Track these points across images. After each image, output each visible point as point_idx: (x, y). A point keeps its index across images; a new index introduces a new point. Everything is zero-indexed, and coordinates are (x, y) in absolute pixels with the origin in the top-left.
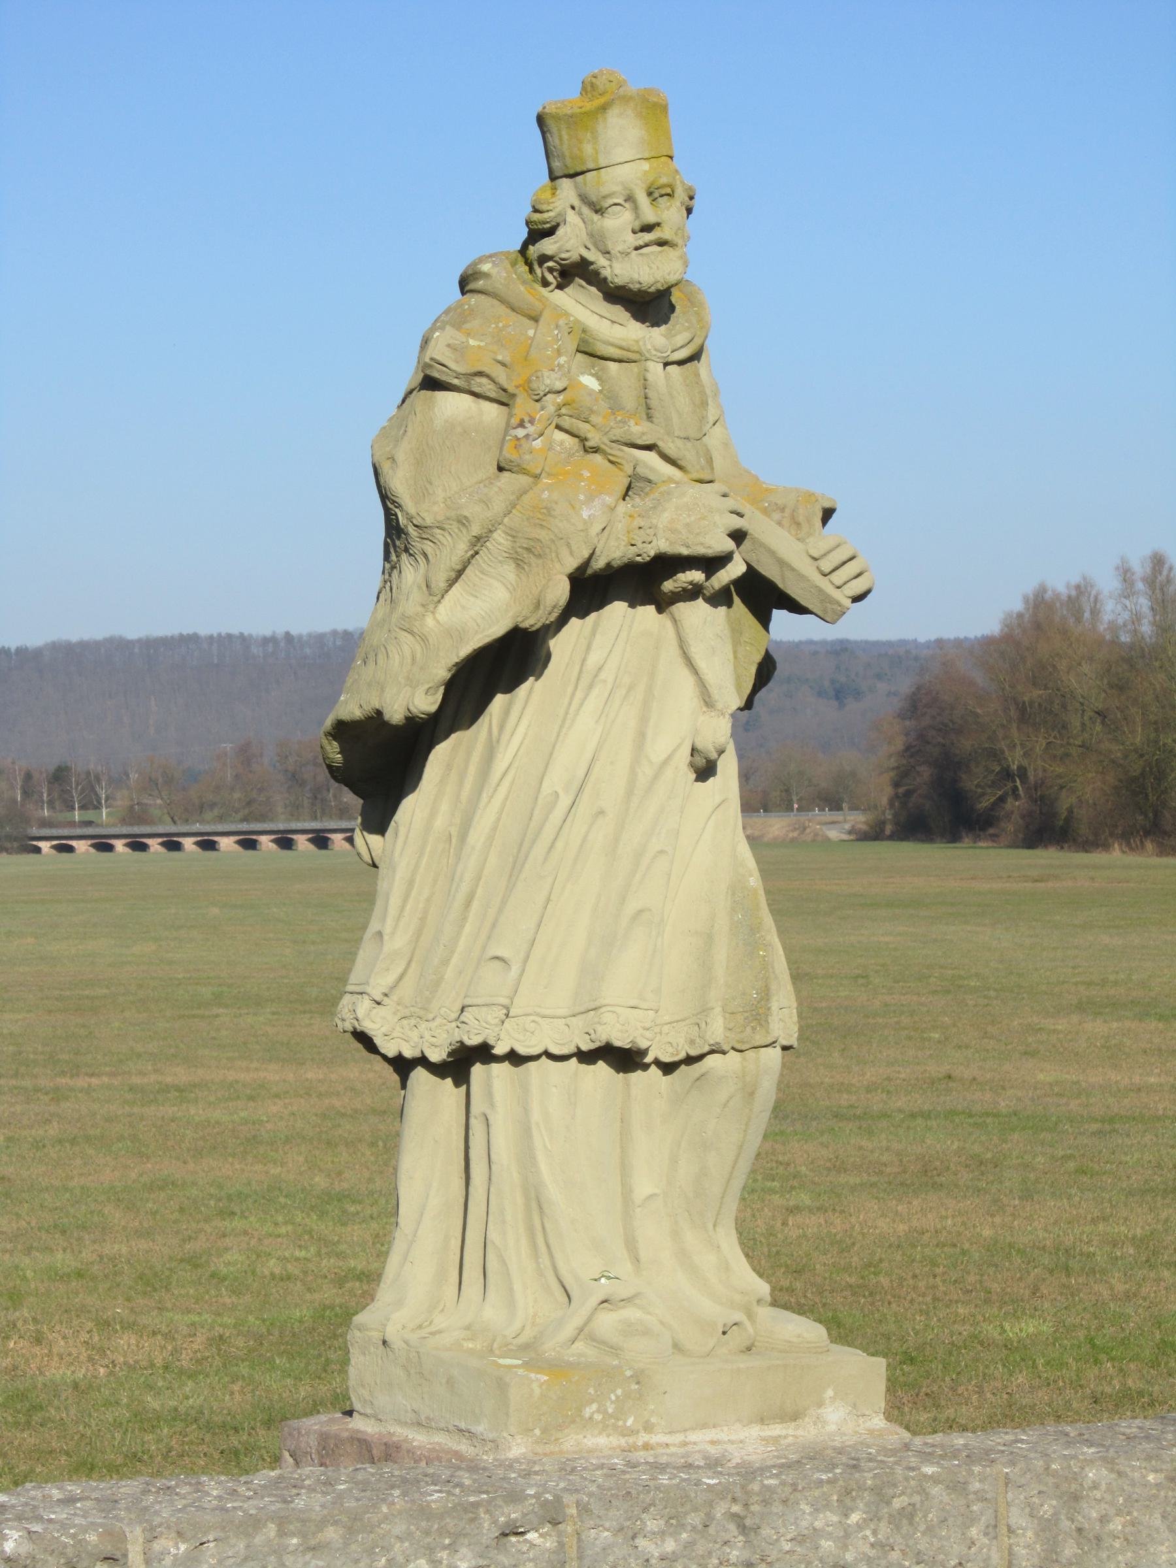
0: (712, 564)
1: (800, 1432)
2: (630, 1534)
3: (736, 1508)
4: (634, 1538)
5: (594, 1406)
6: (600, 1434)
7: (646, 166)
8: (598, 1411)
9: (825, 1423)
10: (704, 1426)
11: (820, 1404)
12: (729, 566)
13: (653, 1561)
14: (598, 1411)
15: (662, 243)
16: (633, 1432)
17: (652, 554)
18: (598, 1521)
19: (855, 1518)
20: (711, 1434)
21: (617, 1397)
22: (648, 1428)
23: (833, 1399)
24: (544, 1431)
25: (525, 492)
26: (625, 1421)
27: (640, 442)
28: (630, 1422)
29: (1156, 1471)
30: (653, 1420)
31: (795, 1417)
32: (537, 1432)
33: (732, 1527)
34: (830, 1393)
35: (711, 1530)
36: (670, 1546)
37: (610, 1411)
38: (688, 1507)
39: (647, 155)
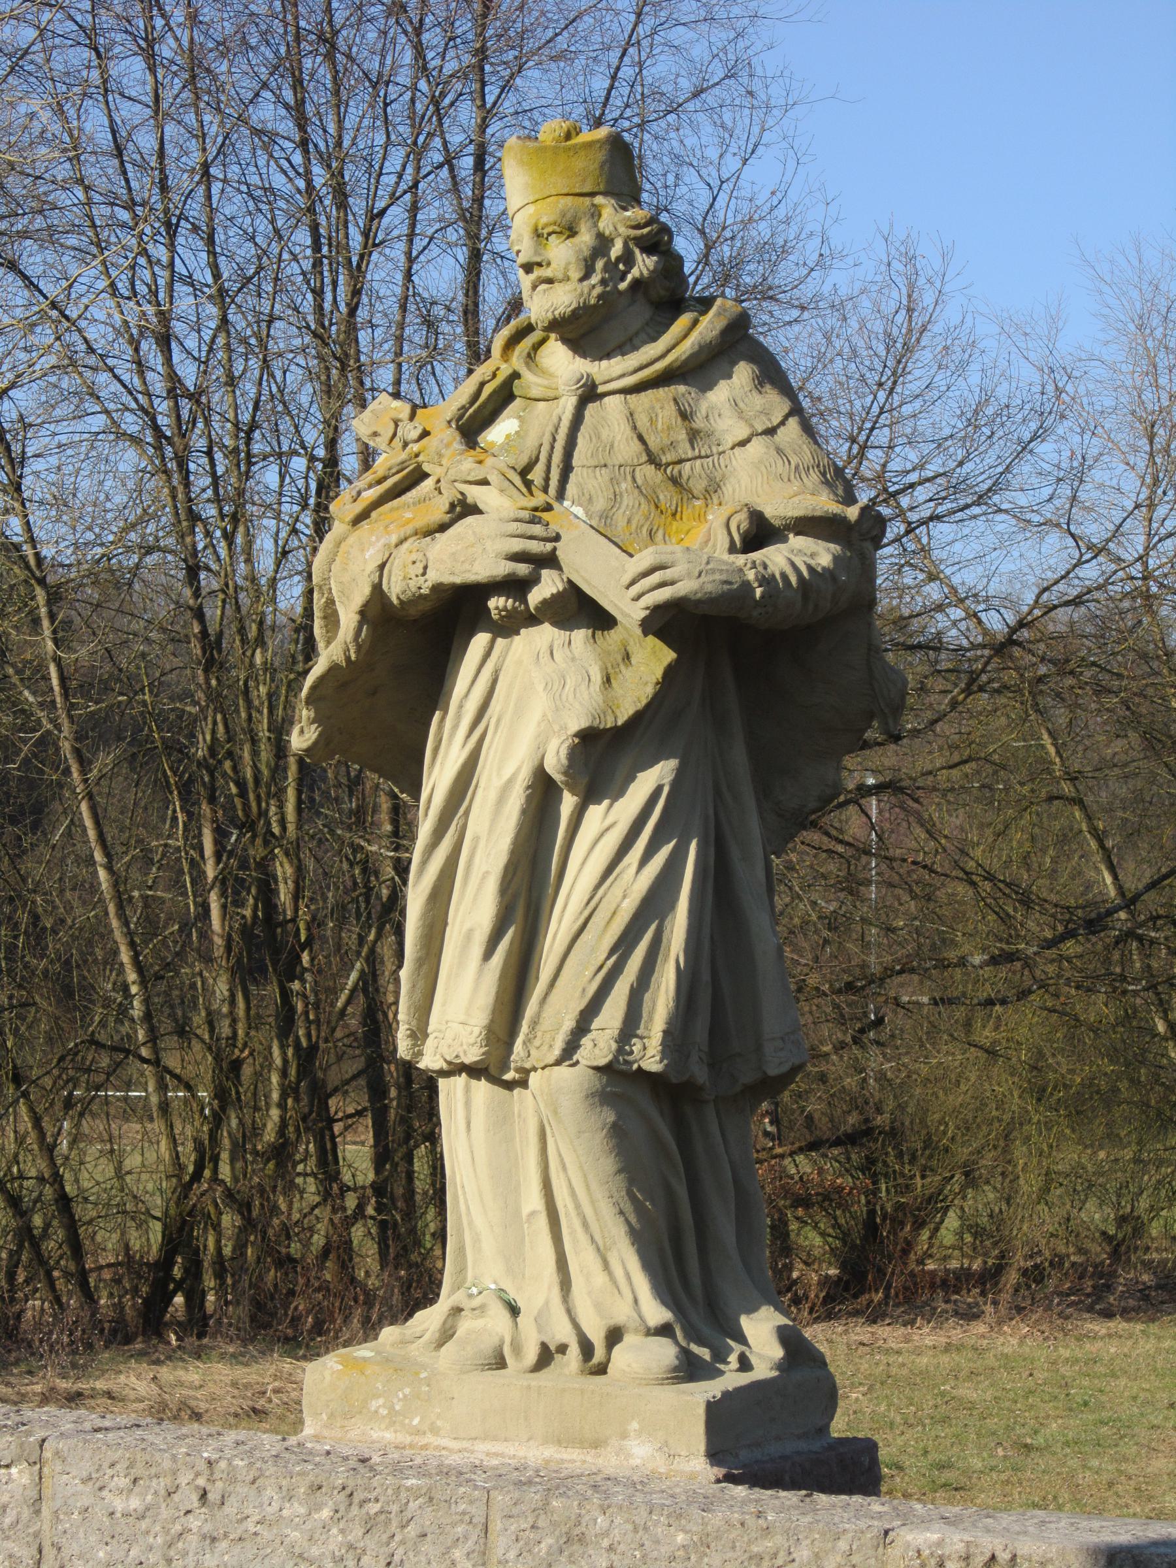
0: (517, 587)
1: (600, 1461)
2: (98, 1485)
3: (201, 1482)
4: (101, 1489)
5: (381, 1401)
6: (387, 1428)
7: (531, 209)
8: (384, 1406)
9: (629, 1456)
10: (495, 1439)
11: (624, 1436)
12: (535, 590)
13: (119, 1515)
14: (384, 1406)
15: (550, 281)
16: (418, 1432)
17: (429, 584)
18: (68, 1469)
19: (326, 1513)
20: (498, 1447)
21: (405, 1396)
22: (435, 1430)
23: (639, 1433)
24: (332, 1416)
25: (345, 539)
26: (412, 1420)
27: (470, 478)
28: (416, 1421)
29: (686, 1532)
30: (439, 1423)
31: (597, 1444)
32: (324, 1416)
33: (195, 1497)
34: (635, 1425)
35: (176, 1497)
36: (135, 1503)
37: (397, 1408)
38: (153, 1471)
39: (532, 199)
